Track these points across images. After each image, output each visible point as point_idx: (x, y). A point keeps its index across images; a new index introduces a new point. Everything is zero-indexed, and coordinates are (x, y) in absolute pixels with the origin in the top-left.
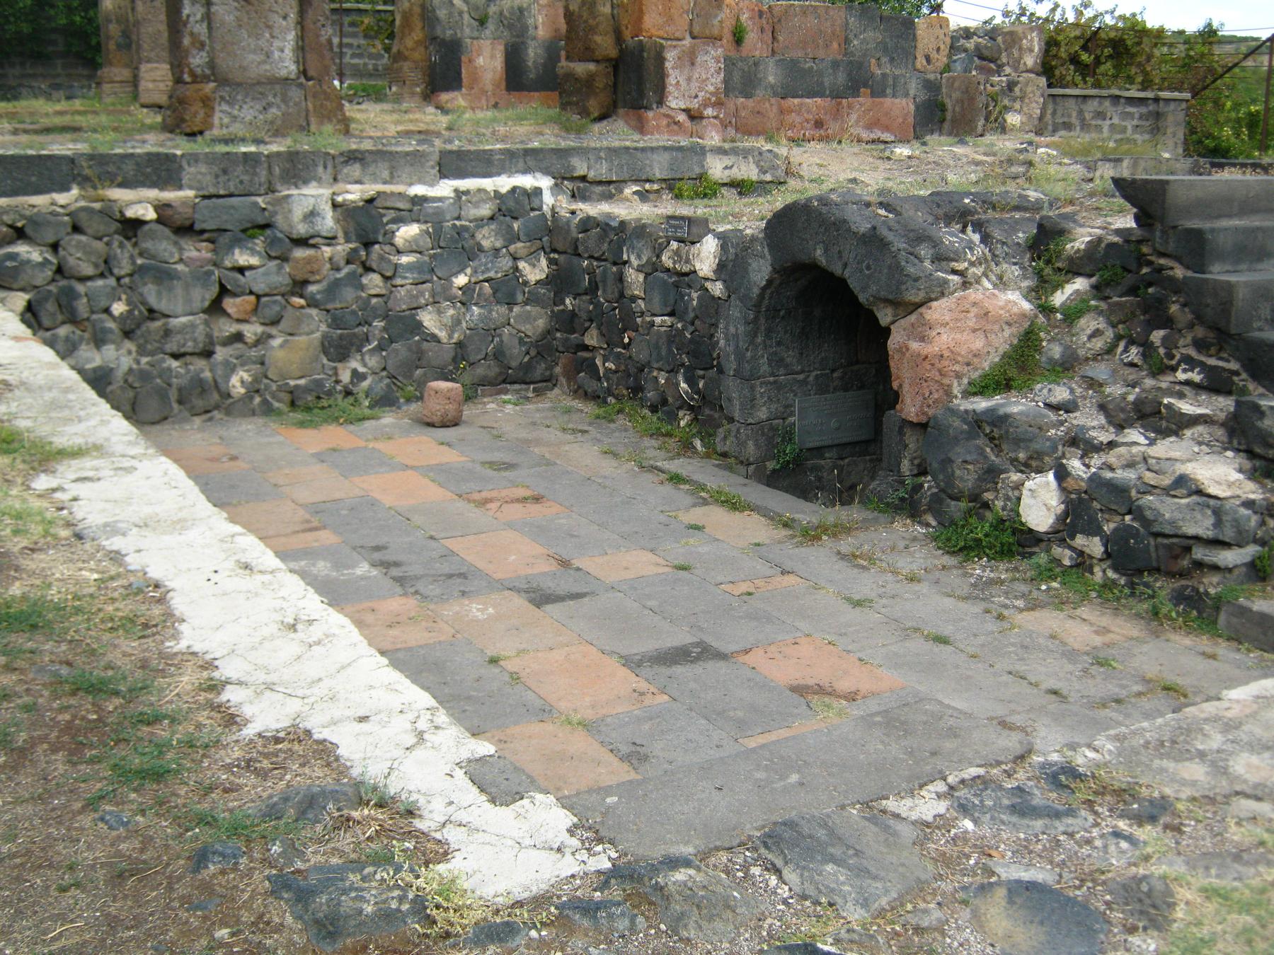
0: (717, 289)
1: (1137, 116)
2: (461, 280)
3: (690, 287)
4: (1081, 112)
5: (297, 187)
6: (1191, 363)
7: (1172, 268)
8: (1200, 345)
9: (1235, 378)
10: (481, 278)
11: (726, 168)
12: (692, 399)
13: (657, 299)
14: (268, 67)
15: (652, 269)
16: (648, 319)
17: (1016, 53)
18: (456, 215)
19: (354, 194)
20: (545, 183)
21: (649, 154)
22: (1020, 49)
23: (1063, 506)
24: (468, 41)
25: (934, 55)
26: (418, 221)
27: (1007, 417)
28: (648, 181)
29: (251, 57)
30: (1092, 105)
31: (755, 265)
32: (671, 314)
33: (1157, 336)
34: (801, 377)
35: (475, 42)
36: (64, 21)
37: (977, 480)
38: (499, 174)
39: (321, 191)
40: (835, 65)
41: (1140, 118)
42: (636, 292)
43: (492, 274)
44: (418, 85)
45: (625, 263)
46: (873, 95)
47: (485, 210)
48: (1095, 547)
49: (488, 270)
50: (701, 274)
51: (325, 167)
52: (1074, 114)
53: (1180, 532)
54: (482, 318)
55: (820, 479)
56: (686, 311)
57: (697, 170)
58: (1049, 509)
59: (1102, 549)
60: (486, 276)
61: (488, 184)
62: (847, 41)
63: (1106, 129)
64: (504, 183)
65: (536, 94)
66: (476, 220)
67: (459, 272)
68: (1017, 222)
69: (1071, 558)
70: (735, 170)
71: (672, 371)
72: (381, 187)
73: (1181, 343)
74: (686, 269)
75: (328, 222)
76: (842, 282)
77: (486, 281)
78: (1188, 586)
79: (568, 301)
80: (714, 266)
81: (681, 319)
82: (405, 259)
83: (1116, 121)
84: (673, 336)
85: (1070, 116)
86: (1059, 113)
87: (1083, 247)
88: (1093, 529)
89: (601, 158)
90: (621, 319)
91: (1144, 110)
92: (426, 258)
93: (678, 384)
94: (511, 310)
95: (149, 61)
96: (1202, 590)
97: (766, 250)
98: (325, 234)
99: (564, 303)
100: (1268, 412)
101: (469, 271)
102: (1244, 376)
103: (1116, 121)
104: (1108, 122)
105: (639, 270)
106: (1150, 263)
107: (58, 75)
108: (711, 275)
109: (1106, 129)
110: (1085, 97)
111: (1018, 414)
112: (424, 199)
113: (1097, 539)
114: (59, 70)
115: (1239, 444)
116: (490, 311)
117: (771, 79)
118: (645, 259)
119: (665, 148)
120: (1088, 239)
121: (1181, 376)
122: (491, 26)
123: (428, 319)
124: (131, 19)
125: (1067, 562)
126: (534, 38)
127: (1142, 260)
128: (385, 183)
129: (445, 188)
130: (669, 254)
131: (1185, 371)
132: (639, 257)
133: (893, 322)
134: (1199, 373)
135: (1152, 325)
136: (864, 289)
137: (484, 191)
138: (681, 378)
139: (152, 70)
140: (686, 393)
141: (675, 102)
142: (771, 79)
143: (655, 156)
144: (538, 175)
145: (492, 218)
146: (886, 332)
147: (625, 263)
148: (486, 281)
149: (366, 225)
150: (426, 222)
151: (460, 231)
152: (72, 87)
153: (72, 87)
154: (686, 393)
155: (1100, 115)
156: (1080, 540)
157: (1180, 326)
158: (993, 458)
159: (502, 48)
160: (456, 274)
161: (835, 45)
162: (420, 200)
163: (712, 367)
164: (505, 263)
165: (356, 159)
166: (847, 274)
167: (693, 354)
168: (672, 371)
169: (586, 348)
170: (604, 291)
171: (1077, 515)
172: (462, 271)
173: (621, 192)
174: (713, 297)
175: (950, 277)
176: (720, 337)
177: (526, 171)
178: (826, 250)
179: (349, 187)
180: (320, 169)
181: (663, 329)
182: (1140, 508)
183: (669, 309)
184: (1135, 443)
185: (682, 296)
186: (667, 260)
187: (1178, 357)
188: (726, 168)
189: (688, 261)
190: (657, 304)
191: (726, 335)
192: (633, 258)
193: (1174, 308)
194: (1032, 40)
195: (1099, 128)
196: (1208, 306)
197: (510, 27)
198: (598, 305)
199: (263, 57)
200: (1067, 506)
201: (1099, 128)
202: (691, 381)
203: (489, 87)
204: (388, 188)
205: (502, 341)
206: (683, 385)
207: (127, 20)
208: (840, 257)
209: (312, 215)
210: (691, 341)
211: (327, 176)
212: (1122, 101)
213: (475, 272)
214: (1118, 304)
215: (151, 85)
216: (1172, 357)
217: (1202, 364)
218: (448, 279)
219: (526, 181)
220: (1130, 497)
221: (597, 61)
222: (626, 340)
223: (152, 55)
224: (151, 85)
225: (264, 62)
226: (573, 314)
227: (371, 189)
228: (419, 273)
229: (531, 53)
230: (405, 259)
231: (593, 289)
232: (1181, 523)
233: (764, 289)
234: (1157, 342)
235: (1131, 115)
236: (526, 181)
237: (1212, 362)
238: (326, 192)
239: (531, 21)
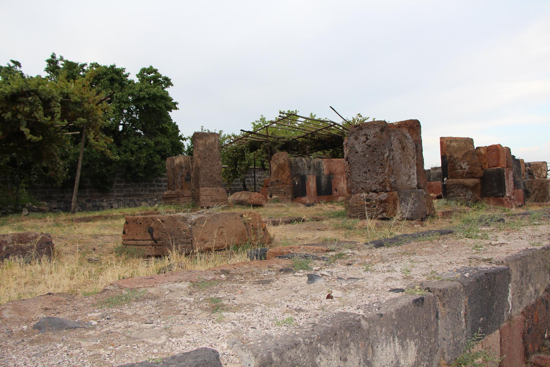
14: (409, 183)
17: (539, 172)
22: (541, 170)
29: (404, 177)
36: (98, 171)
44: (289, 194)
65: (325, 196)
95: (202, 187)
107: (87, 196)
114: (88, 194)
122: (312, 170)
124: (191, 167)
126: (323, 174)
139: (205, 190)
141: (507, 194)
152: (95, 201)
153: (95, 201)
159: (315, 178)
197: (316, 170)
199: (407, 178)
203: (313, 195)
207: (189, 168)
215: (205, 198)
221: (477, 178)
223: (204, 183)
224: (205, 198)
225: (408, 180)
229: (323, 180)
239: (322, 167)
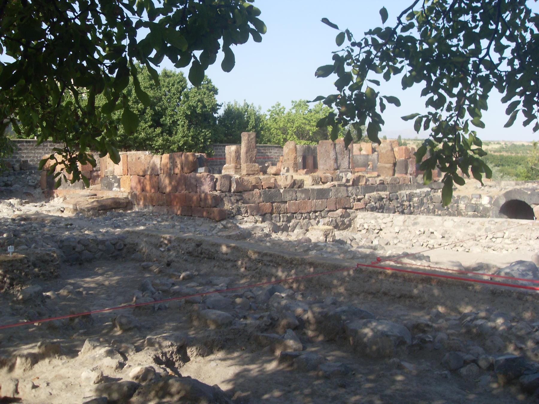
2: (422, 209)
13: (469, 209)
19: (408, 192)
74: (479, 203)
75: (405, 198)
129: (418, 191)
149: (410, 198)
162: (416, 193)
164: (428, 205)
186: (473, 202)
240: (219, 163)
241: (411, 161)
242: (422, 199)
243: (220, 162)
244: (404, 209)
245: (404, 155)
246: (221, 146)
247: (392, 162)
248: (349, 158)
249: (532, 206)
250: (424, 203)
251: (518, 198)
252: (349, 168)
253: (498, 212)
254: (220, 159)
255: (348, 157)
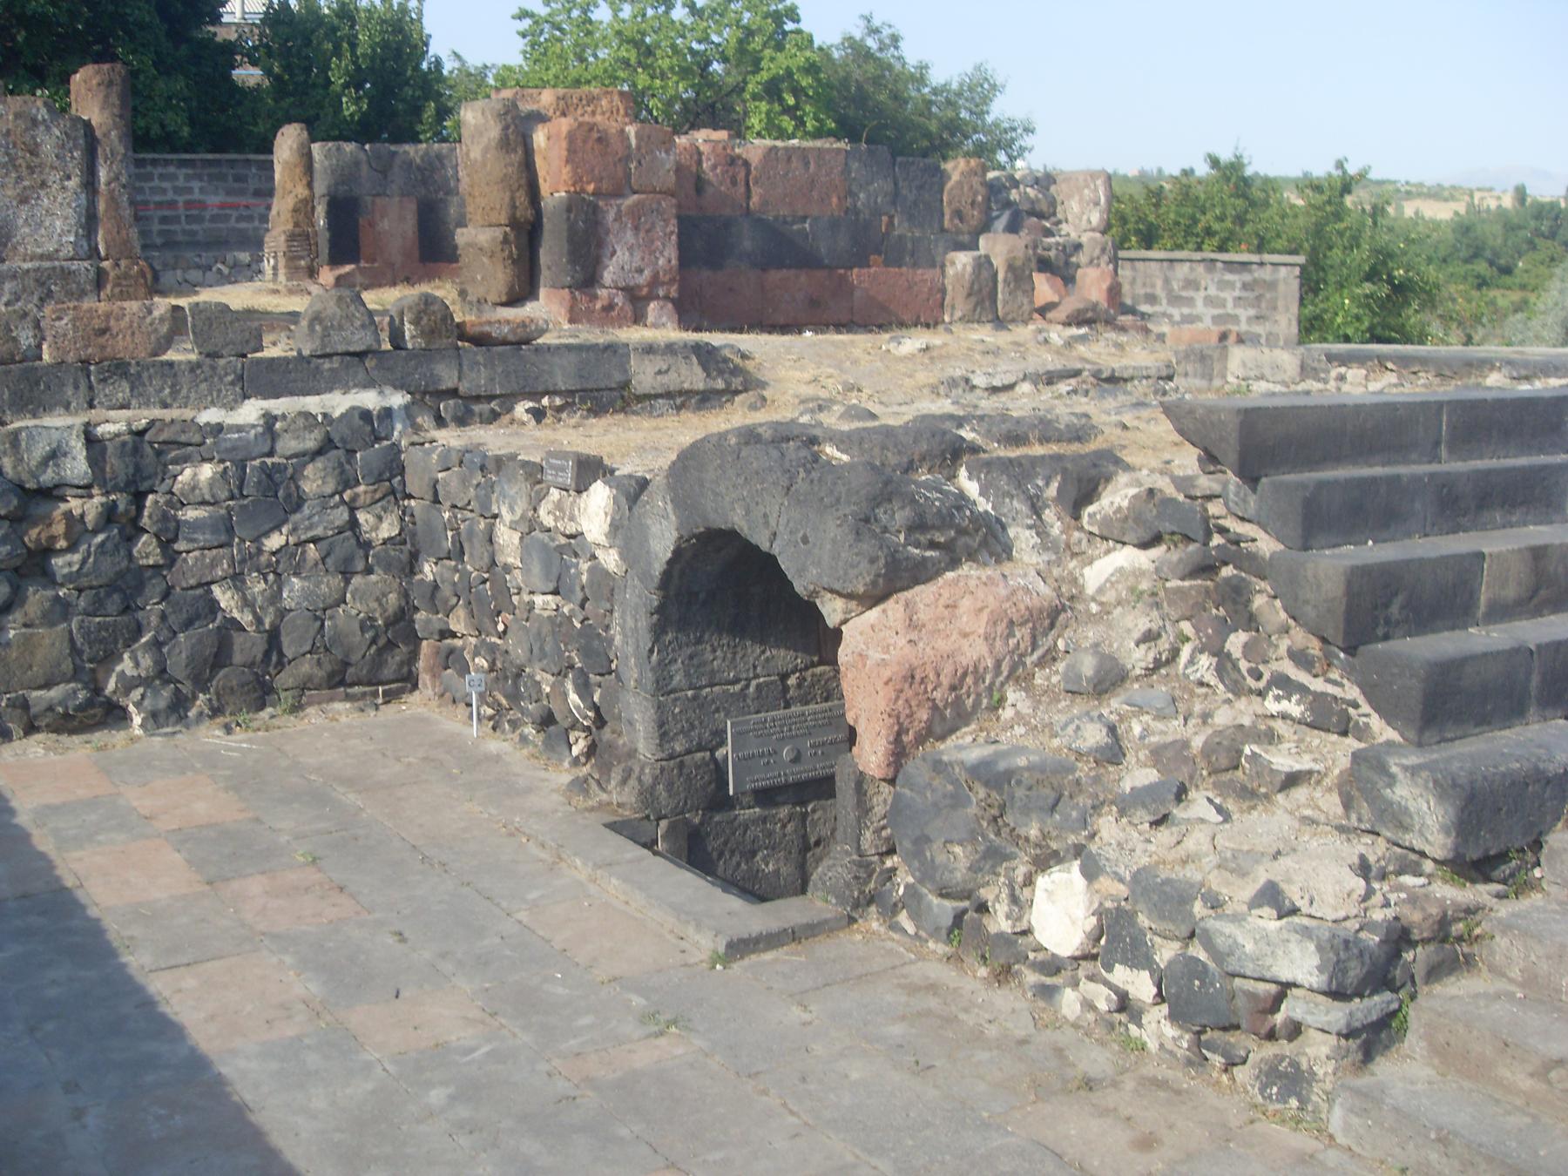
0: (610, 560)
1: (1238, 285)
2: (275, 541)
3: (576, 555)
4: (1167, 281)
5: (35, 416)
6: (1284, 684)
7: (1254, 540)
8: (1300, 658)
9: (1351, 710)
10: (303, 537)
11: (660, 372)
12: (586, 717)
13: (536, 568)
15: (530, 526)
16: (526, 598)
18: (266, 449)
19: (113, 424)
20: (398, 400)
21: (548, 356)
23: (1094, 920)
24: (369, 199)
25: (967, 210)
26: (210, 460)
27: (1009, 774)
28: (547, 393)
30: (1182, 270)
31: (655, 529)
32: (556, 592)
33: (1236, 642)
34: (738, 687)
35: (378, 200)
37: (970, 869)
38: (330, 390)
39: (69, 421)
40: (834, 224)
41: (1245, 286)
42: (510, 560)
43: (319, 531)
44: (302, 258)
45: (495, 516)
46: (887, 264)
47: (311, 442)
48: (1141, 986)
49: (310, 528)
50: (590, 537)
51: (76, 387)
52: (1159, 283)
53: (1268, 975)
54: (306, 595)
55: (770, 834)
56: (572, 591)
57: (618, 377)
58: (1074, 923)
59: (1155, 990)
60: (310, 534)
61: (312, 403)
62: (851, 193)
63: (1200, 303)
64: (338, 403)
66: (295, 456)
67: (272, 530)
68: (1034, 461)
69: (1108, 999)
70: (673, 375)
71: (560, 674)
72: (157, 413)
73: (1272, 654)
74: (571, 529)
75: (77, 466)
76: (770, 561)
77: (314, 540)
78: (1283, 1058)
79: (427, 568)
80: (606, 528)
81: (567, 599)
82: (191, 514)
83: (1212, 291)
84: (559, 622)
85: (1153, 286)
86: (1139, 282)
87: (1125, 504)
88: (1139, 957)
89: (478, 363)
90: (494, 597)
91: (1247, 277)
92: (223, 512)
93: (566, 695)
94: (347, 582)
96: (1304, 1066)
97: (670, 507)
98: (76, 482)
99: (421, 572)
100: (1401, 776)
101: (284, 530)
102: (1365, 708)
103: (1212, 291)
104: (1202, 293)
105: (513, 527)
106: (1223, 531)
108: (602, 540)
109: (1200, 303)
110: (1171, 261)
111: (1029, 768)
112: (218, 429)
113: (1146, 974)
115: (1360, 820)
116: (318, 585)
117: (747, 245)
118: (519, 512)
119: (569, 347)
120: (1133, 491)
121: (1272, 706)
123: (224, 597)
125: (1103, 1006)
127: (1209, 527)
128: (165, 406)
129: (250, 412)
130: (550, 506)
131: (1278, 698)
132: (512, 509)
133: (845, 622)
134: (1298, 703)
135: (1225, 628)
136: (801, 571)
137: (307, 415)
138: (569, 686)
140: (577, 708)
142: (747, 245)
143: (556, 359)
144: (388, 390)
145: (319, 452)
146: (837, 635)
147: (495, 516)
148: (314, 540)
149: (136, 469)
150: (222, 461)
151: (269, 473)
154: (577, 708)
155: (1191, 284)
156: (1120, 975)
157: (1269, 629)
158: (992, 836)
160: (267, 534)
161: (835, 200)
163: (610, 673)
164: (342, 515)
165: (125, 375)
166: (776, 551)
167: (586, 652)
168: (560, 674)
169: (453, 635)
170: (471, 555)
171: (1114, 938)
172: (277, 528)
173: (510, 410)
174: (607, 573)
175: (929, 554)
176: (616, 631)
177: (368, 384)
178: (748, 512)
179: (112, 413)
180: (70, 391)
181: (546, 614)
182: (1206, 931)
183: (551, 586)
184: (1202, 821)
185: (568, 568)
187: (1266, 676)
188: (660, 372)
189: (572, 519)
190: (537, 581)
191: (623, 628)
192: (504, 511)
193: (1259, 602)
194: (1096, 190)
195: (1190, 302)
196: (1306, 602)
198: (465, 575)
200: (1100, 920)
201: (1190, 302)
202: (584, 689)
204: (168, 414)
205: (335, 626)
206: (573, 698)
208: (767, 523)
209: (55, 455)
210: (581, 633)
211: (77, 399)
212: (1219, 265)
213: (294, 530)
214: (1178, 590)
216: (1258, 676)
217: (1303, 689)
218: (256, 540)
219: (369, 399)
220: (1191, 914)
222: (501, 627)
226: (435, 587)
227: (141, 417)
228: (213, 533)
230: (191, 514)
231: (459, 553)
232: (1269, 961)
233: (670, 562)
234: (1237, 653)
235: (1231, 285)
236: (369, 399)
237: (1317, 685)
238: (78, 421)
240: (159, 241)
241: (636, 213)
242: (269, 473)
243: (161, 233)
244: (48, 551)
245: (566, 172)
246: (167, 163)
247: (503, 219)
248: (90, 184)
249: (832, 610)
250: (298, 502)
251: (737, 520)
252: (93, 253)
253: (644, 623)
254: (164, 220)
255: (72, 184)
